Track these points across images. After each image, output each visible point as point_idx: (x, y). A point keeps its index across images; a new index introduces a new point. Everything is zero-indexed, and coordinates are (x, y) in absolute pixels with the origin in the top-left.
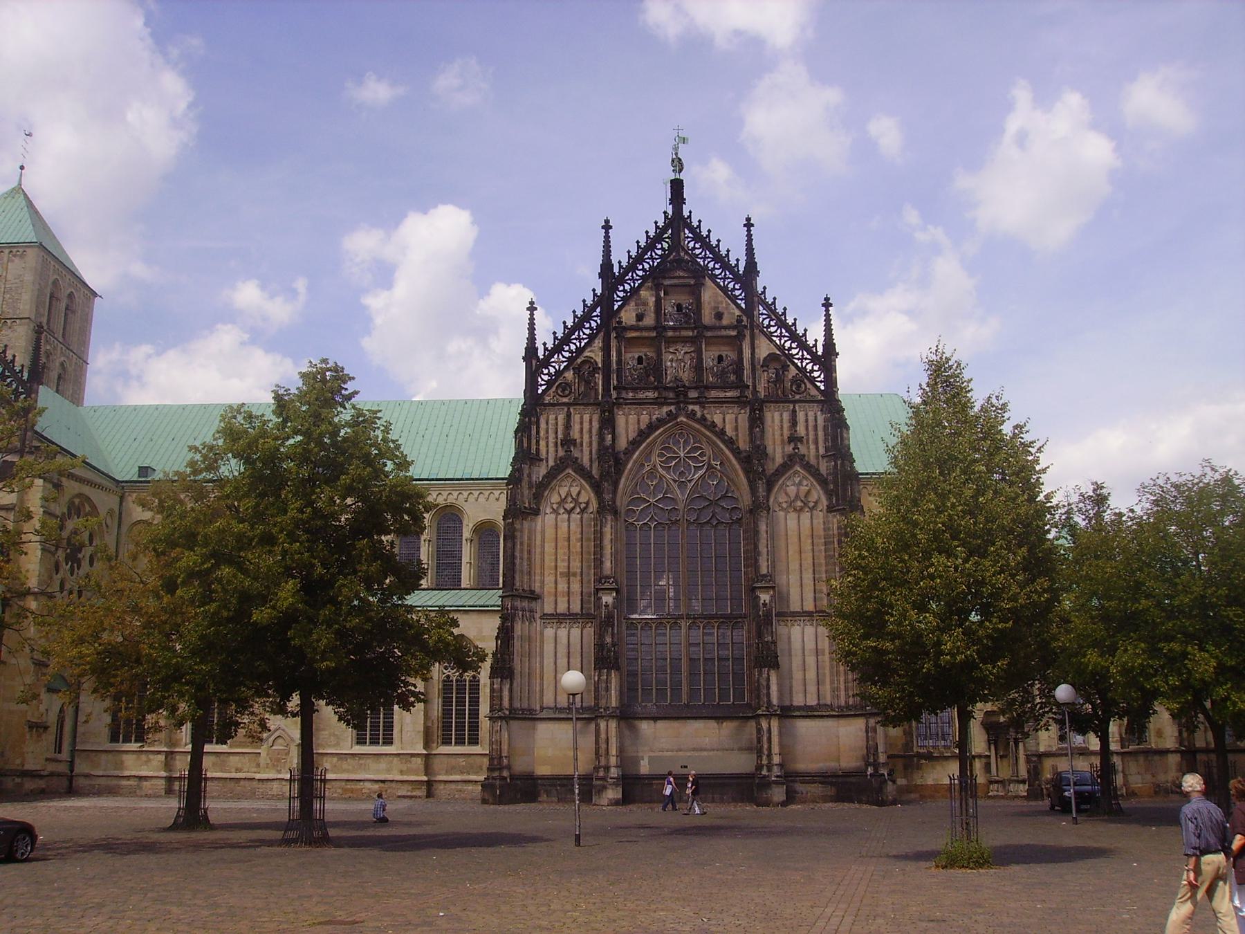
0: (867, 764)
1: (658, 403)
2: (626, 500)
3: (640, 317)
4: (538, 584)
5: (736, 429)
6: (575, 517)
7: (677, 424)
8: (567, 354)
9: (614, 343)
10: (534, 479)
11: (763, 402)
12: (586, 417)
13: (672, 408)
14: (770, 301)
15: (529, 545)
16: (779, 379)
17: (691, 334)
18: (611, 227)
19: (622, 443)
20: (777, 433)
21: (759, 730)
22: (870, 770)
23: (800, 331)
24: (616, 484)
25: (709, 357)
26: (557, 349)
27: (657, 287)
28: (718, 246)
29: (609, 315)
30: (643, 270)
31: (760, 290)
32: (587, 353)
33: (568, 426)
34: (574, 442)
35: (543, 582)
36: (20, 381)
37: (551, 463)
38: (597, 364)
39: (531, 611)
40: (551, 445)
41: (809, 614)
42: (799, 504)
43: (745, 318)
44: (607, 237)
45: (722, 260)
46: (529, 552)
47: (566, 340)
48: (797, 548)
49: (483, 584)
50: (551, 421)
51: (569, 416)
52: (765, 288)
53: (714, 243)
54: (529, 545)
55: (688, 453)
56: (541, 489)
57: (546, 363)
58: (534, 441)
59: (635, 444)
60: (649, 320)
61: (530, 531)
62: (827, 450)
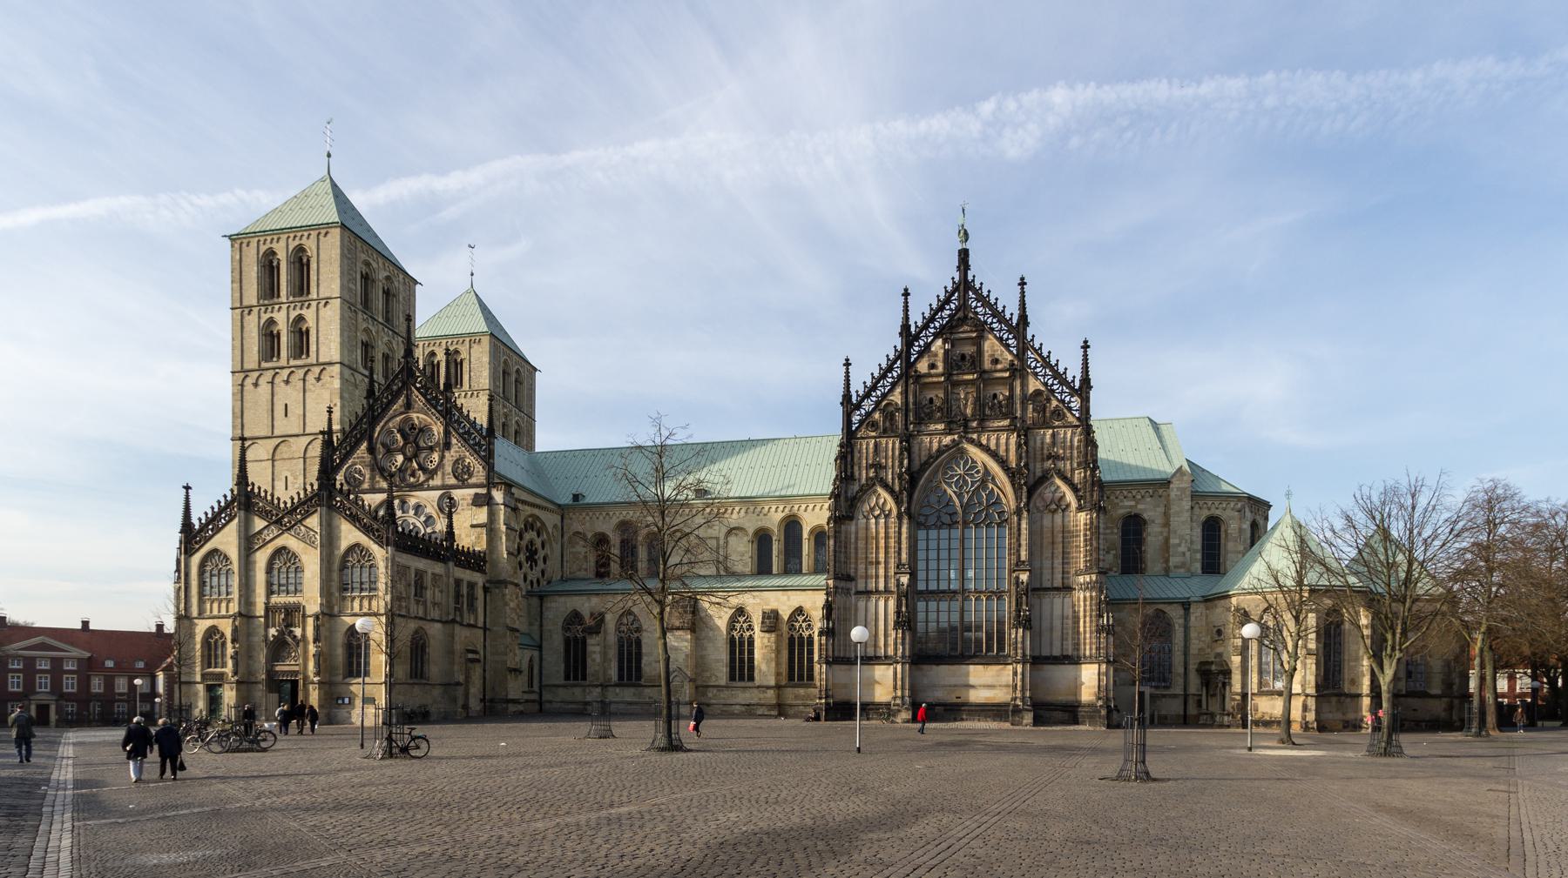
0: (1099, 698)
3: (932, 366)
4: (852, 570)
5: (1007, 450)
6: (882, 521)
7: (959, 449)
8: (874, 399)
9: (912, 387)
10: (849, 495)
11: (1028, 428)
13: (956, 437)
14: (1037, 346)
15: (846, 543)
16: (1042, 409)
17: (971, 377)
18: (909, 294)
20: (1038, 453)
21: (1015, 673)
22: (1100, 703)
23: (1061, 370)
24: (910, 497)
26: (867, 395)
27: (945, 341)
28: (996, 303)
29: (909, 366)
30: (935, 328)
31: (1029, 338)
35: (856, 569)
37: (863, 481)
38: (896, 404)
39: (848, 589)
41: (1057, 589)
42: (1054, 506)
43: (1016, 362)
44: (906, 303)
45: (999, 315)
46: (846, 547)
47: (874, 388)
48: (1050, 540)
49: (816, 571)
51: (876, 445)
52: (1033, 336)
53: (993, 301)
54: (846, 543)
55: (967, 470)
57: (858, 406)
58: (849, 466)
60: (940, 369)
61: (846, 532)
62: (1079, 464)
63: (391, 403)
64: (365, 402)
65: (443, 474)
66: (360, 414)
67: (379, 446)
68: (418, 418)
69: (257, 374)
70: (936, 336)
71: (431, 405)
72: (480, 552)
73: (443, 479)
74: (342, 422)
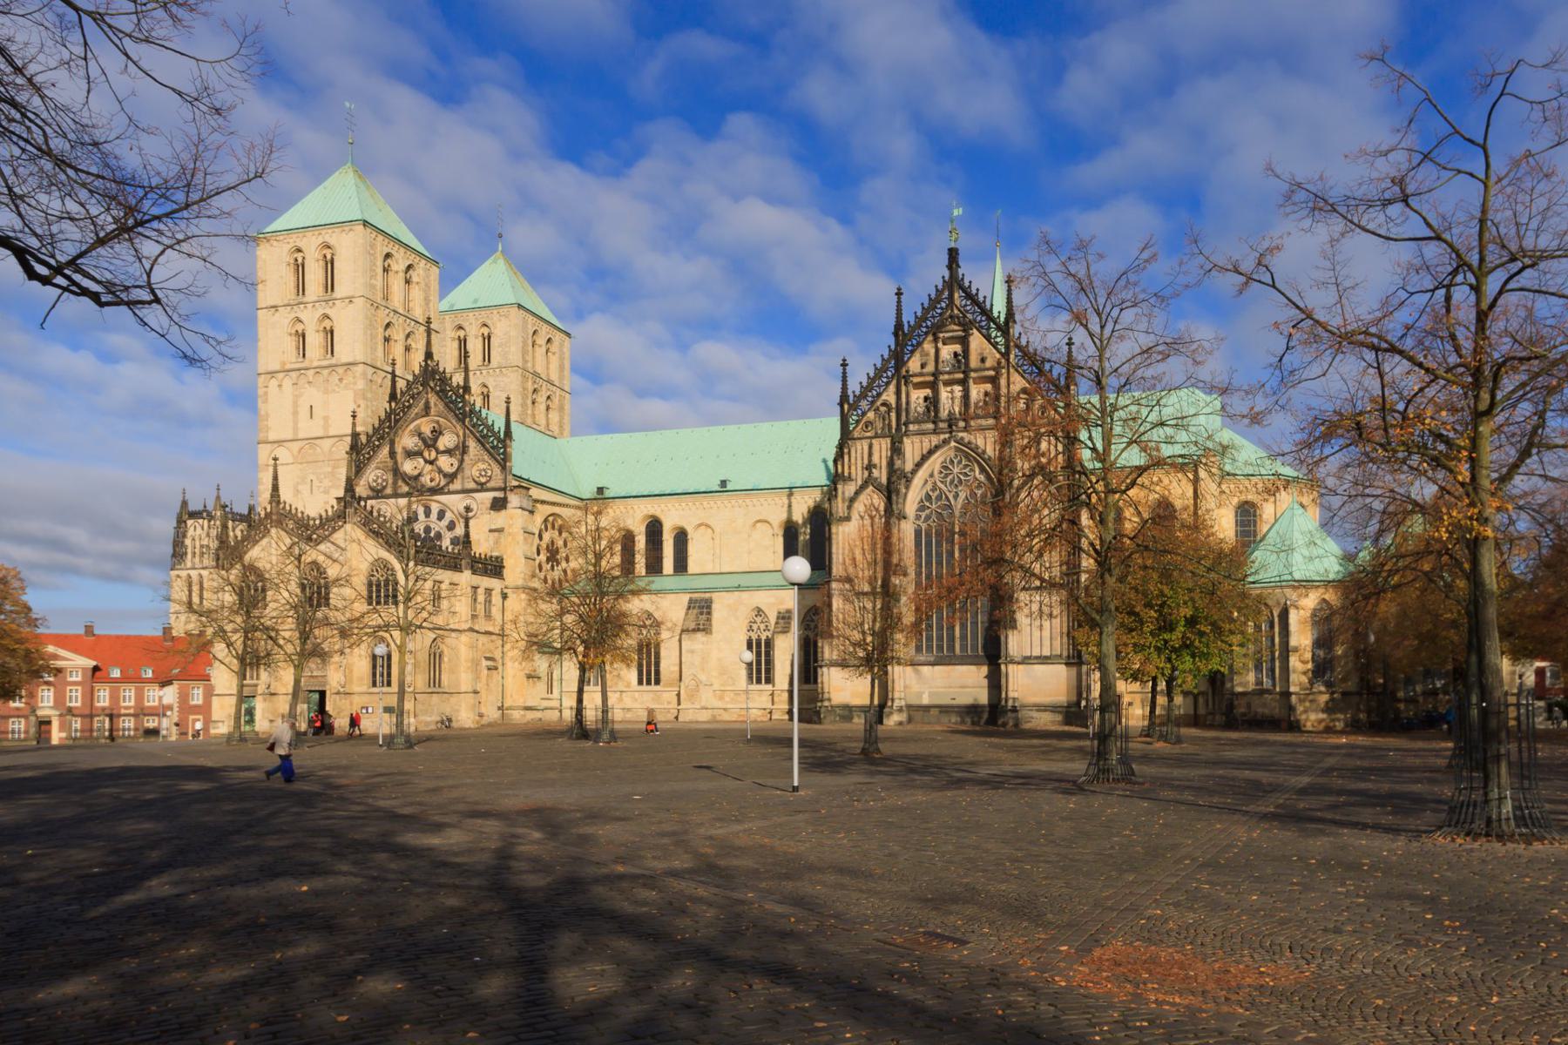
1: (935, 432)
2: (915, 506)
3: (923, 366)
9: (903, 388)
12: (884, 446)
13: (947, 436)
14: (1024, 342)
19: (909, 466)
25: (976, 392)
26: (863, 396)
27: (936, 340)
30: (927, 327)
32: (884, 397)
33: (870, 454)
34: (875, 466)
36: (499, 440)
37: (860, 482)
40: (859, 468)
44: (899, 302)
50: (859, 452)
51: (870, 447)
56: (852, 500)
59: (918, 465)
60: (930, 368)
63: (409, 407)
64: (387, 406)
65: (463, 478)
66: (383, 417)
67: (399, 450)
68: (438, 422)
69: (281, 375)
70: (926, 334)
71: (450, 409)
72: (497, 558)
73: (463, 483)
74: (364, 424)
